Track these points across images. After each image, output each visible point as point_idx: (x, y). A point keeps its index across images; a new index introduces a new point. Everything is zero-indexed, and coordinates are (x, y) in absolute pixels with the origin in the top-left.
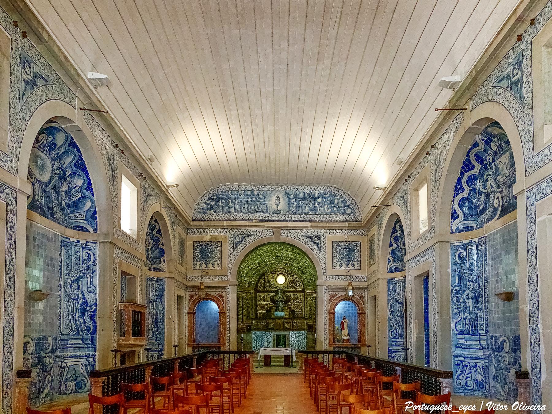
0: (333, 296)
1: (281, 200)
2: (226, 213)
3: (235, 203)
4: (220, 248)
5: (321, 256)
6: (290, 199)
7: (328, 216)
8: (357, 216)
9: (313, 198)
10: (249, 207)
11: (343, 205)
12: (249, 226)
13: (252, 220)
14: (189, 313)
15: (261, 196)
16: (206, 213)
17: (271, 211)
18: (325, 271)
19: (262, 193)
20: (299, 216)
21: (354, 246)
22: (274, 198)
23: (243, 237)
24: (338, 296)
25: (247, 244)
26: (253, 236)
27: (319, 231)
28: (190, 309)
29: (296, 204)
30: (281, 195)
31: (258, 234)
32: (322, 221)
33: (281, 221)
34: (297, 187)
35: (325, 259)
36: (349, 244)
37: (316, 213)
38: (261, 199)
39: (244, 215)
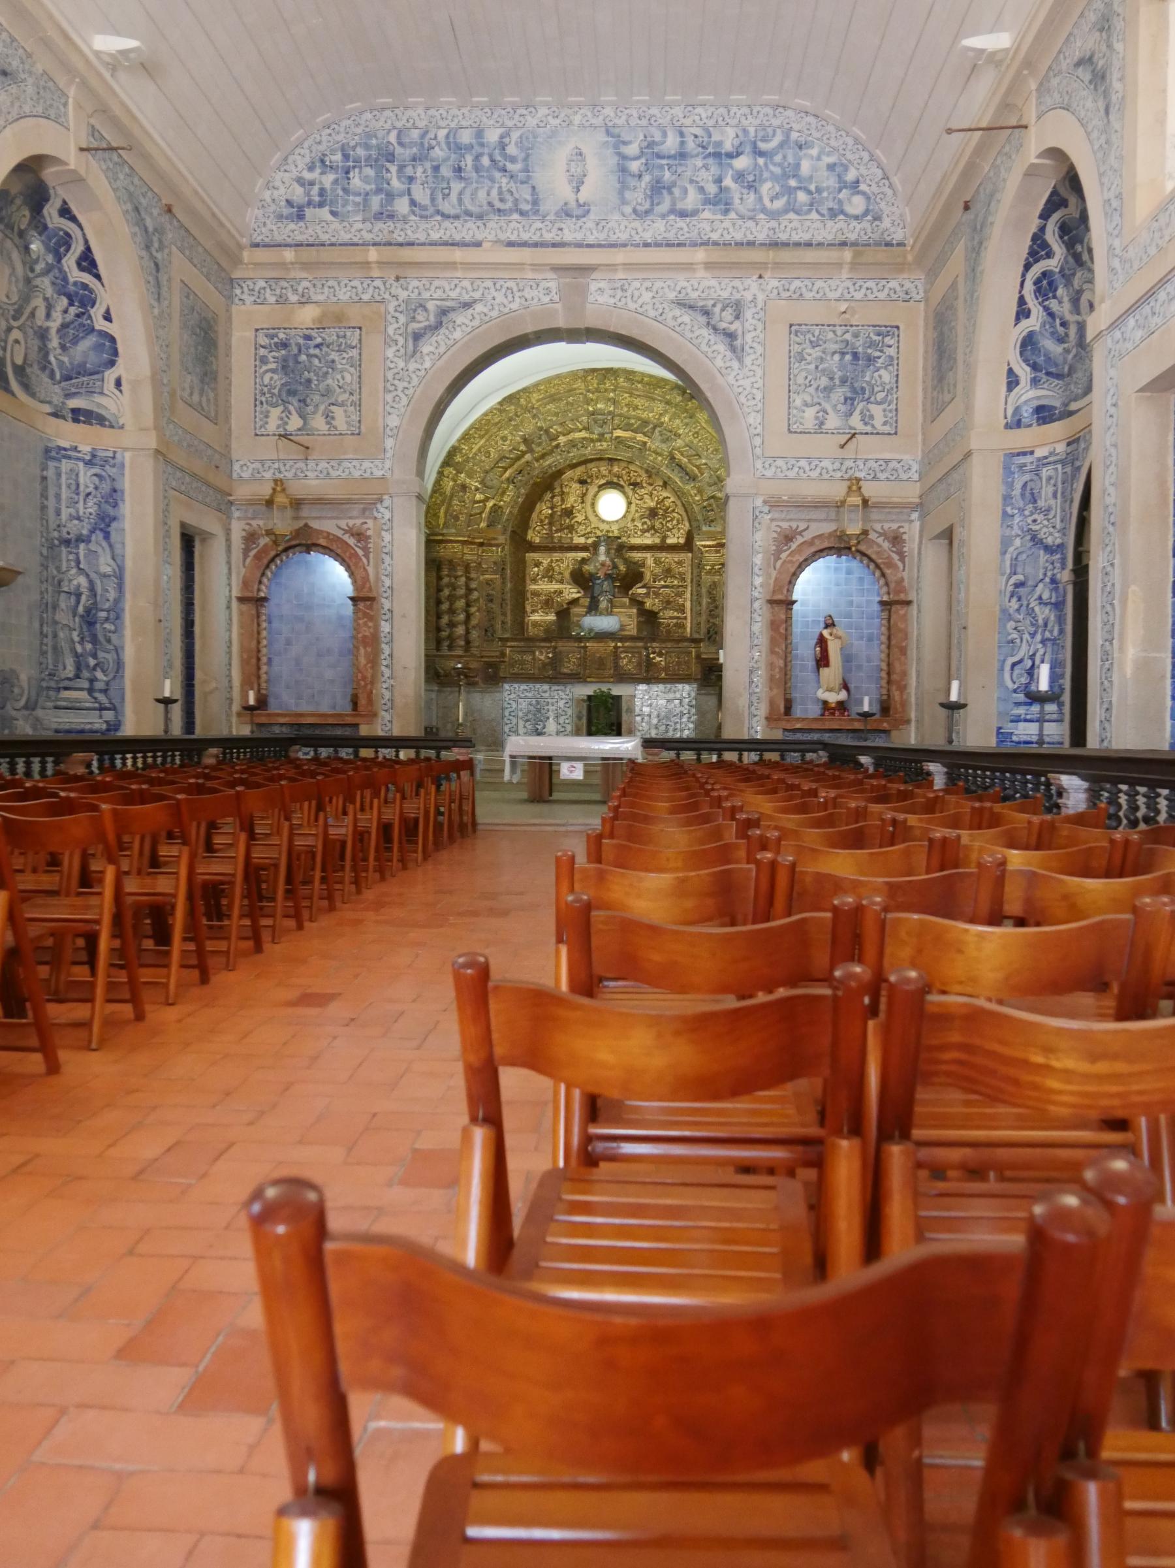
0: (788, 538)
1: (592, 162)
2: (379, 216)
3: (411, 179)
4: (354, 353)
5: (747, 383)
6: (624, 157)
7: (774, 224)
8: (886, 223)
9: (717, 155)
10: (468, 192)
11: (832, 182)
12: (468, 266)
13: (478, 244)
14: (241, 600)
15: (511, 150)
16: (300, 217)
17: (549, 206)
18: (757, 441)
19: (515, 135)
20: (660, 225)
21: (872, 344)
22: (562, 155)
23: (444, 312)
24: (808, 536)
25: (457, 334)
26: (479, 308)
27: (737, 283)
28: (245, 584)
29: (647, 178)
30: (592, 144)
31: (500, 298)
32: (751, 244)
33: (589, 246)
34: (654, 111)
35: (759, 396)
36: (856, 336)
37: (726, 212)
38: (513, 160)
39: (447, 224)
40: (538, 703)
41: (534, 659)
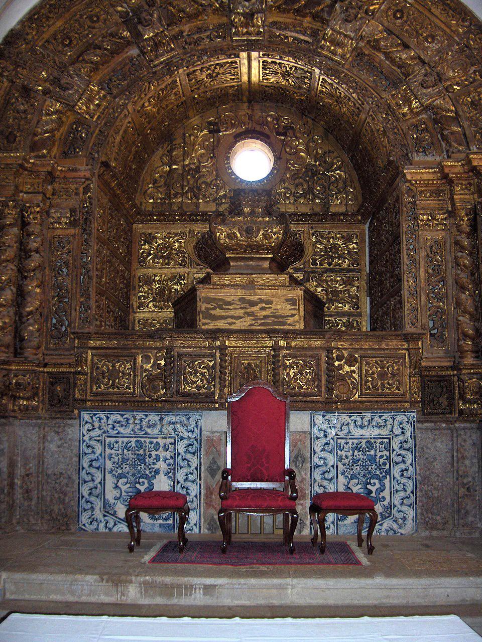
40: (140, 445)
41: (134, 368)
